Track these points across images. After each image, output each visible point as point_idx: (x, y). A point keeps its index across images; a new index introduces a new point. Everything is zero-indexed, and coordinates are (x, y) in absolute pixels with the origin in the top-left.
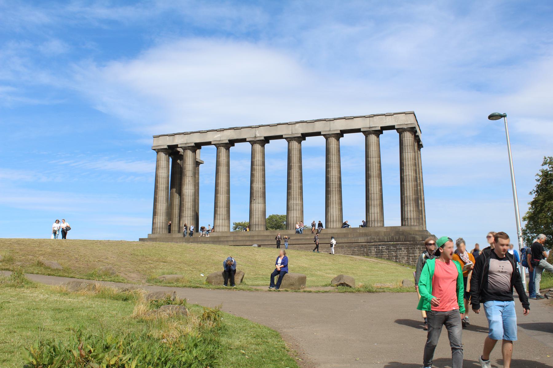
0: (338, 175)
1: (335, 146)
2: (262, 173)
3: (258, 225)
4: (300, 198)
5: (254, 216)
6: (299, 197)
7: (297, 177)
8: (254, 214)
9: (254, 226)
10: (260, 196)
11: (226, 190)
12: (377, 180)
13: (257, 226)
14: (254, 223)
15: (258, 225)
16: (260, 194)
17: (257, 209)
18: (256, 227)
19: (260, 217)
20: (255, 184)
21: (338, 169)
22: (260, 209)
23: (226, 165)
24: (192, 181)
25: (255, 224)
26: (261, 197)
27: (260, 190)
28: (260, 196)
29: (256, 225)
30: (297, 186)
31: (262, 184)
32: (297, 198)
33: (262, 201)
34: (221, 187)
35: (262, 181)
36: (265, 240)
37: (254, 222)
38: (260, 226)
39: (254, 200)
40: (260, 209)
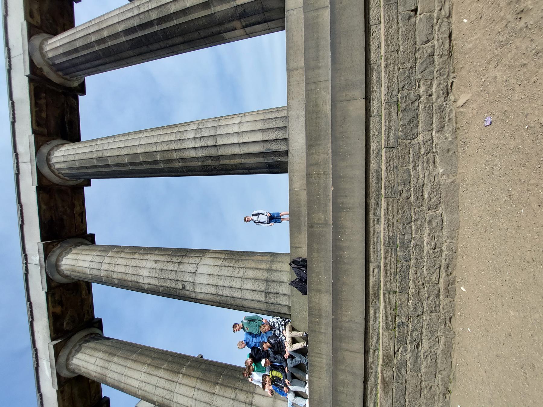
3: (267, 281)
5: (234, 294)
8: (227, 293)
9: (273, 299)
10: (177, 265)
13: (274, 288)
14: (262, 298)
15: (267, 281)
16: (170, 267)
17: (215, 281)
18: (277, 293)
19: (242, 270)
20: (140, 280)
22: (216, 271)
25: (263, 295)
26: (179, 263)
27: (159, 265)
28: (175, 267)
29: (267, 293)
33: (192, 260)
34: (153, 391)
36: (337, 248)
37: (256, 296)
38: (275, 276)
39: (184, 288)
40: (216, 271)
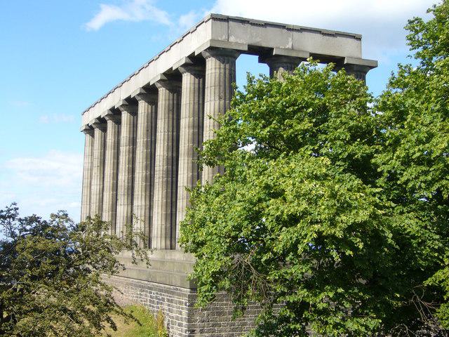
0: (166, 153)
1: (164, 102)
2: (127, 157)
4: (143, 197)
6: (144, 194)
7: (141, 161)
11: (111, 185)
12: (186, 161)
21: (166, 144)
23: (113, 147)
24: (99, 173)
30: (141, 176)
31: (127, 174)
32: (140, 197)
35: (127, 169)
